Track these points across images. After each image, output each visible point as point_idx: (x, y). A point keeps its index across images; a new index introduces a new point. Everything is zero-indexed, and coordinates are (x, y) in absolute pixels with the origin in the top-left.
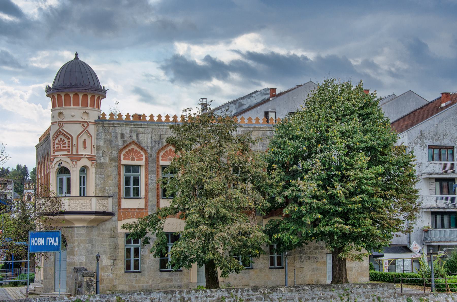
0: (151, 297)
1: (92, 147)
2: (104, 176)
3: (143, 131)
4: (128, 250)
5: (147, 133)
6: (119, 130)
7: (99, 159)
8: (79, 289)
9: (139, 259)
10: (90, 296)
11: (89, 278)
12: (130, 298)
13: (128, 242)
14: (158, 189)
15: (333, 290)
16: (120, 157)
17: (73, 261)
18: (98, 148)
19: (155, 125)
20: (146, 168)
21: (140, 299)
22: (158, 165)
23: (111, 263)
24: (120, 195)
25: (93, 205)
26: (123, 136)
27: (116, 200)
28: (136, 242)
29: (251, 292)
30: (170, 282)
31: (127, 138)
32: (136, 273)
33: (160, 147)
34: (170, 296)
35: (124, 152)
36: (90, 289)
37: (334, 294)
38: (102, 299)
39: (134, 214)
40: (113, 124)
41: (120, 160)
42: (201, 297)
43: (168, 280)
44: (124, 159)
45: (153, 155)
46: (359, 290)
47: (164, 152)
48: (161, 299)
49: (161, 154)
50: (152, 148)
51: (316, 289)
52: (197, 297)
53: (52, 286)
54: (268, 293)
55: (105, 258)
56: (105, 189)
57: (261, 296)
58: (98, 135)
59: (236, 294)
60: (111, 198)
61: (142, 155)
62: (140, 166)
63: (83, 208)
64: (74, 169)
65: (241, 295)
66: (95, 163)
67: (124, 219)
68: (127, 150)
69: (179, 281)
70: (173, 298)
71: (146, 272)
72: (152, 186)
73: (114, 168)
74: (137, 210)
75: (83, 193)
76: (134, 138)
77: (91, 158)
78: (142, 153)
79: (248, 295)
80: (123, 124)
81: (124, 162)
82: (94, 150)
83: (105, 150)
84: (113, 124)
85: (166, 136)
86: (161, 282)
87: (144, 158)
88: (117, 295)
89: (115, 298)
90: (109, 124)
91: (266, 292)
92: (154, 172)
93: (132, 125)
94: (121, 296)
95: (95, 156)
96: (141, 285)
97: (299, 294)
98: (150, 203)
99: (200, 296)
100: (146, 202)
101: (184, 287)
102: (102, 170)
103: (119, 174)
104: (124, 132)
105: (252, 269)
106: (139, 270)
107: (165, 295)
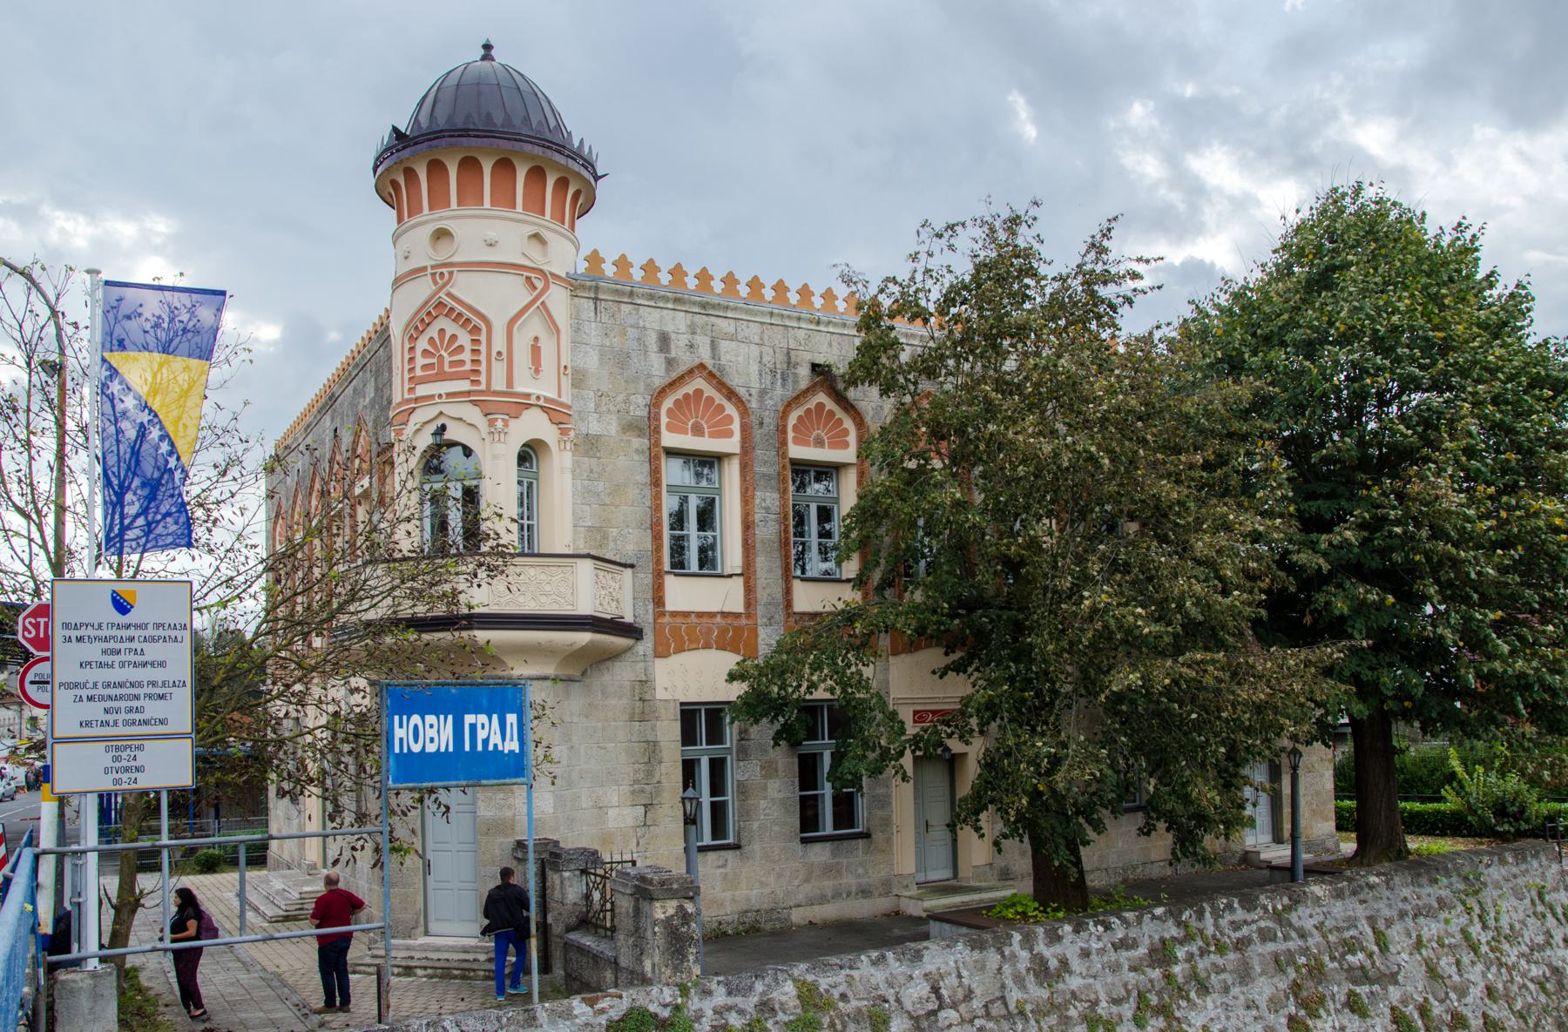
0: (930, 968)
1: (562, 370)
2: (600, 486)
3: (732, 329)
4: (689, 768)
5: (746, 341)
6: (653, 319)
7: (582, 420)
8: (588, 941)
9: (729, 798)
10: (684, 990)
11: (674, 903)
12: (850, 981)
13: (688, 737)
14: (784, 544)
15: (1436, 881)
16: (658, 419)
17: (509, 814)
18: (579, 379)
19: (771, 314)
20: (744, 468)
21: (891, 985)
22: (784, 455)
23: (636, 818)
24: (659, 561)
25: (584, 591)
26: (664, 340)
27: (647, 579)
28: (715, 736)
29: (1240, 914)
31: (678, 349)
32: (723, 853)
33: (790, 394)
34: (993, 958)
35: (668, 403)
36: (684, 957)
37: (1444, 893)
38: (739, 1000)
39: (709, 632)
40: (631, 294)
41: (657, 431)
42: (1102, 951)
43: (829, 870)
44: (670, 428)
45: (767, 420)
46: (1495, 873)
47: (799, 412)
48: (965, 973)
49: (792, 420)
50: (763, 393)
51: (1397, 879)
52: (1085, 954)
53: (418, 914)
54: (1287, 909)
55: (615, 800)
56: (605, 537)
57: (1270, 924)
58: (577, 330)
59: (1200, 926)
60: (629, 571)
61: (730, 419)
62: (707, 461)
63: (543, 599)
64: (499, 448)
65: (1216, 926)
66: (572, 433)
67: (679, 650)
68: (679, 394)
69: (860, 871)
70: (1007, 968)
71: (757, 847)
72: (767, 531)
73: (636, 457)
74: (719, 619)
75: (529, 550)
76: (704, 355)
77: (555, 412)
78: (731, 410)
79: (1236, 926)
80: (667, 300)
81: (670, 439)
82: (566, 382)
83: (604, 389)
84: (631, 294)
85: (805, 358)
86: (807, 880)
87: (736, 427)
88: (796, 972)
89: (790, 988)
90: (616, 292)
91: (1280, 907)
92: (774, 482)
93: (694, 303)
94: (810, 978)
95: (569, 407)
96: (741, 893)
97: (1363, 902)
98: (761, 595)
99: (1095, 945)
100: (749, 590)
101: (876, 893)
102: (594, 461)
103: (656, 482)
104: (669, 328)
106: (731, 840)
107: (976, 955)
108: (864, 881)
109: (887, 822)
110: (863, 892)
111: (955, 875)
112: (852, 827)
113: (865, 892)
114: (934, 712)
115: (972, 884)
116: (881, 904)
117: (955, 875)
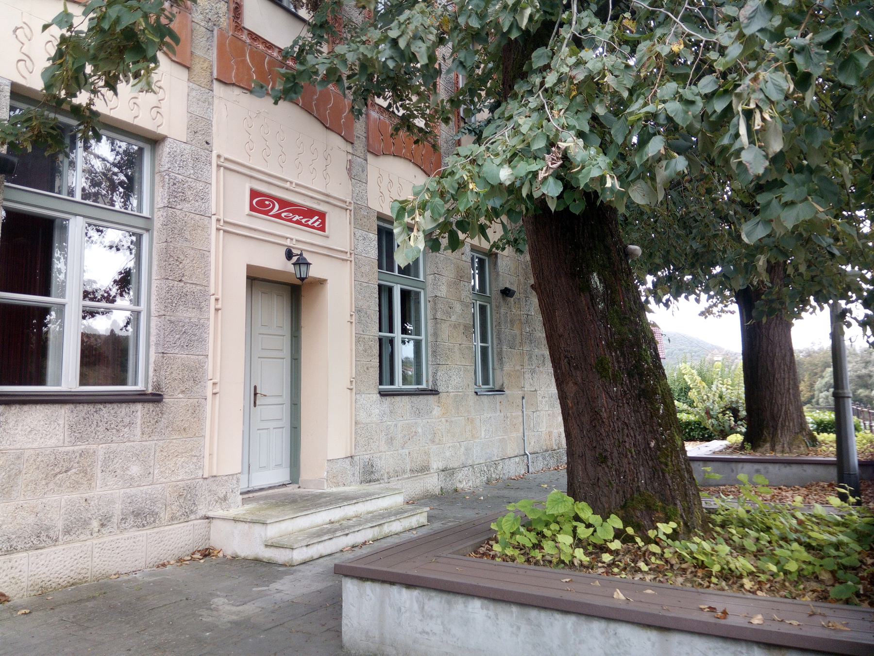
30: (75, 486)
43: (58, 469)
69: (135, 470)
101: (165, 516)
105: (434, 392)
108: (141, 491)
109: (194, 376)
110: (137, 514)
111: (295, 477)
112: (124, 382)
113: (142, 516)
114: (284, 204)
115: (328, 489)
116: (176, 538)
117: (295, 477)
